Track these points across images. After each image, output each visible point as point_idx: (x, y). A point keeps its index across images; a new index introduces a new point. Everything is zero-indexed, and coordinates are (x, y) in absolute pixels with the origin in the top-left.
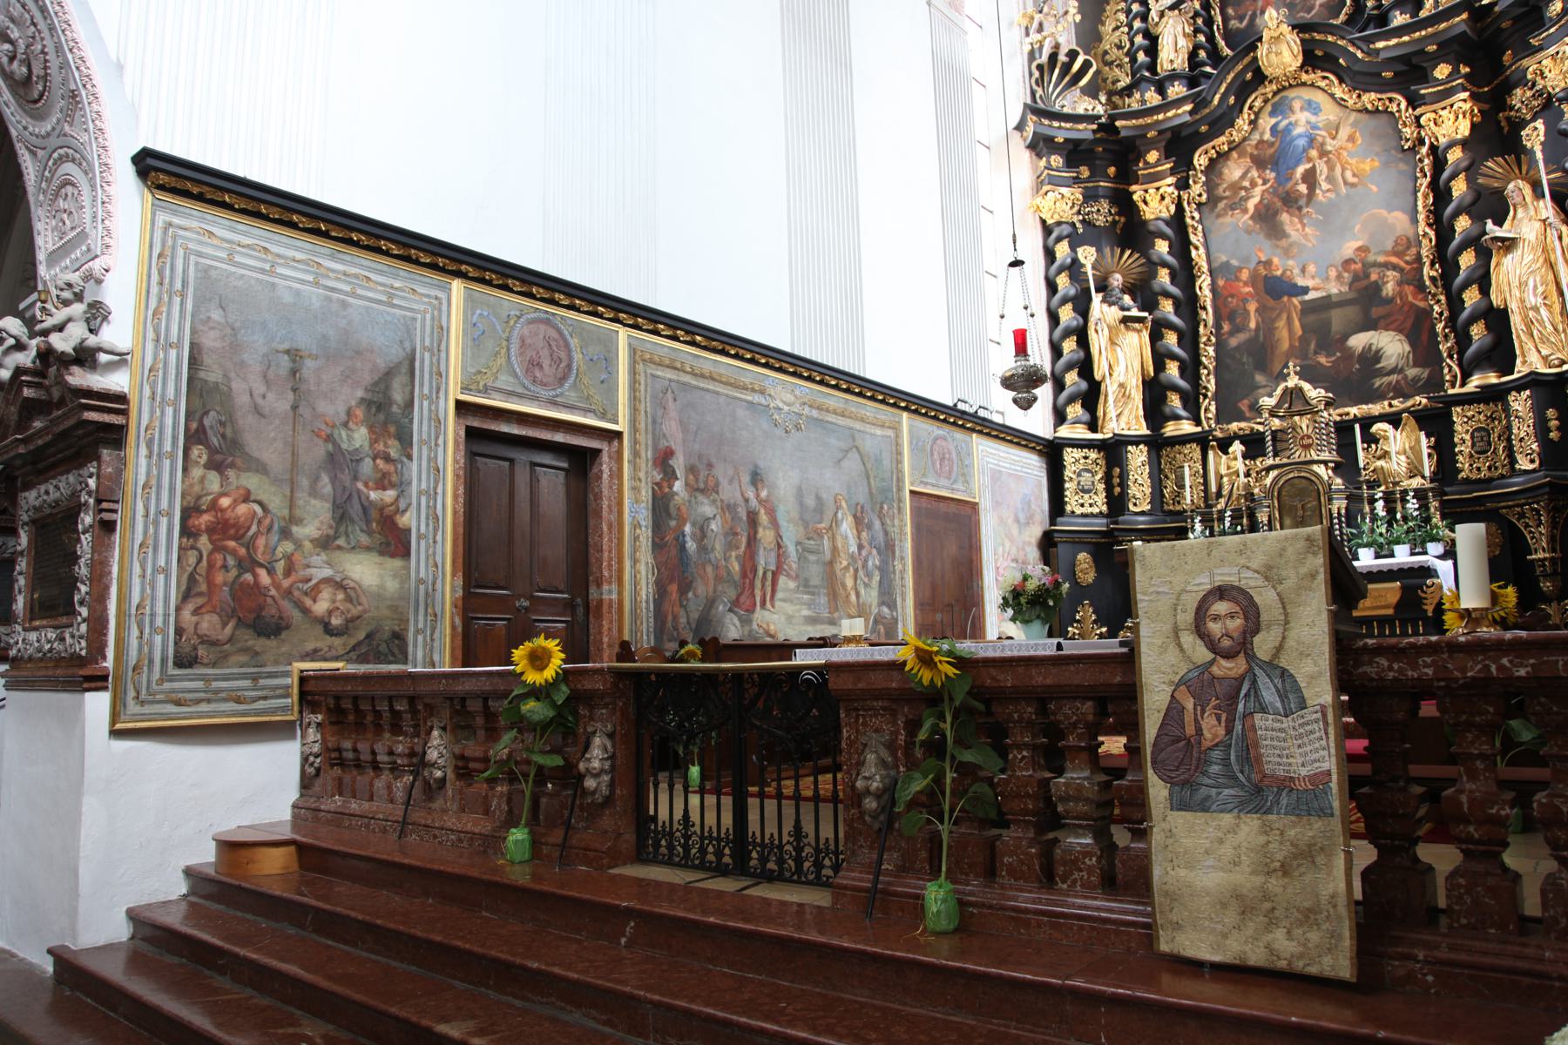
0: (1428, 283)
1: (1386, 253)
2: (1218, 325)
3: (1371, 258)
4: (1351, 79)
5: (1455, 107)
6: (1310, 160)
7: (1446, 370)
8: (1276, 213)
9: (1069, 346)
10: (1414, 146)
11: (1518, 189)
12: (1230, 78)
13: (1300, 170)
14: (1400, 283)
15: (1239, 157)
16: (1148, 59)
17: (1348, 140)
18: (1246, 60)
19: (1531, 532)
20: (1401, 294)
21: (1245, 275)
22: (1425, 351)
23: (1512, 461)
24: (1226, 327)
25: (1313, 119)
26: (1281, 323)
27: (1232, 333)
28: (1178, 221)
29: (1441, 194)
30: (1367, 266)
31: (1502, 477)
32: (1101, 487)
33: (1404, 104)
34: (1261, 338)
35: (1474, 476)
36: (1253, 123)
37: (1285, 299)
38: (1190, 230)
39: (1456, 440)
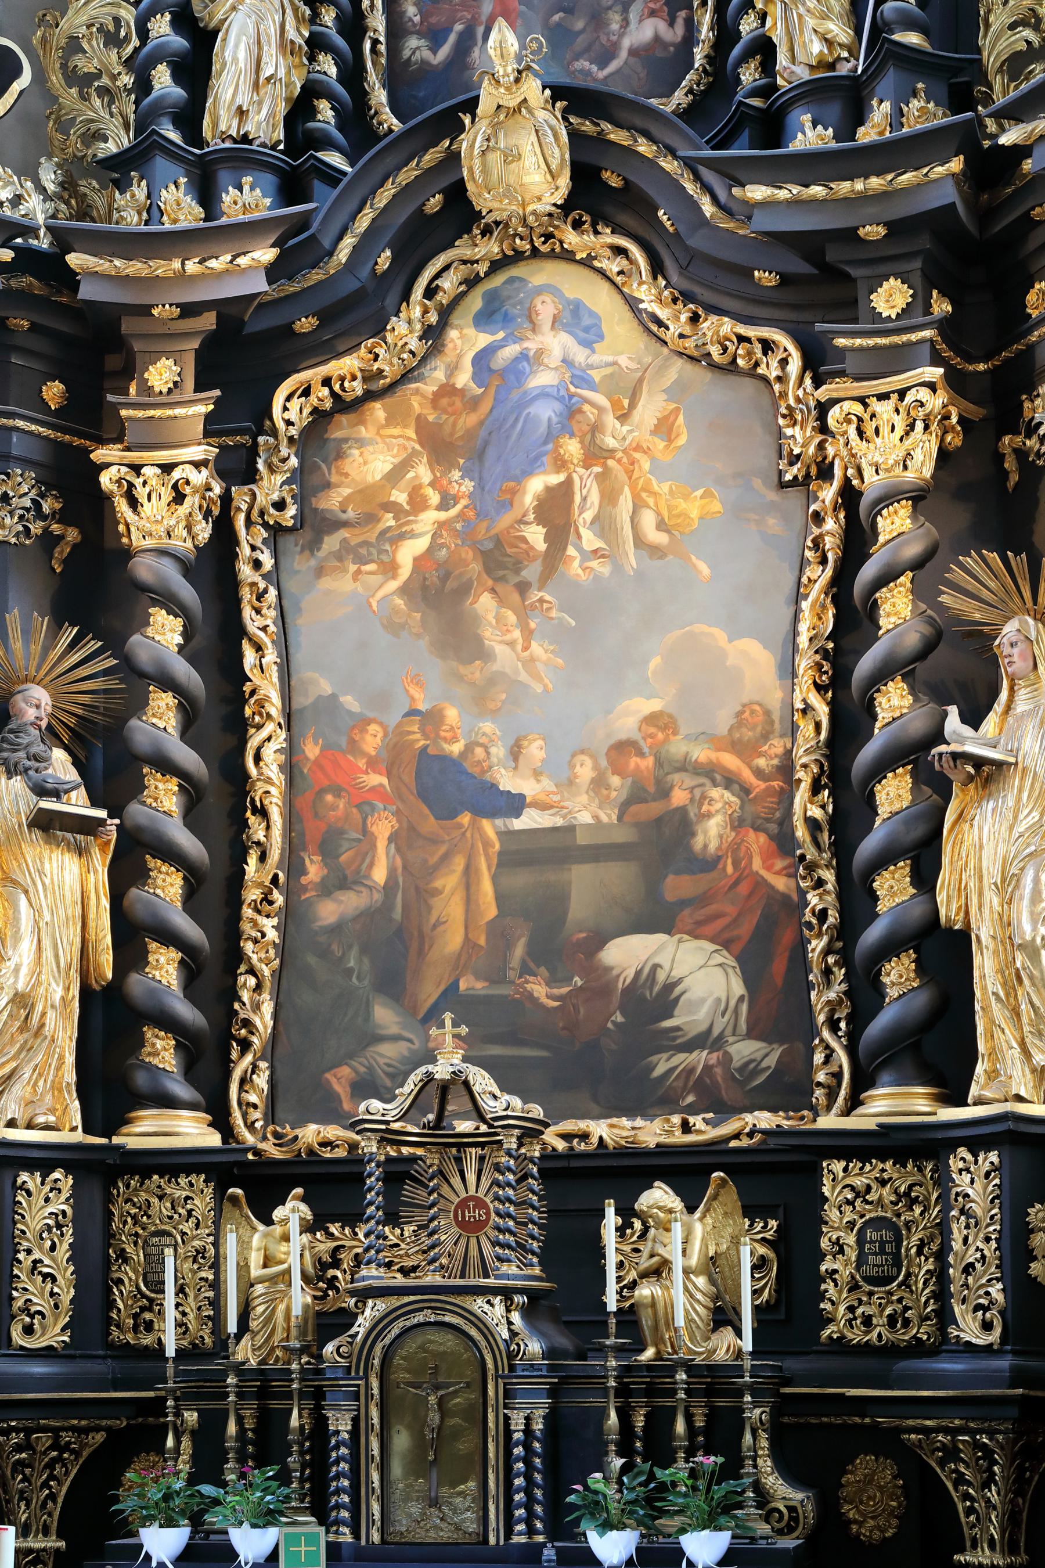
0: (801, 832)
1: (718, 743)
3: (678, 747)
4: (683, 269)
5: (910, 397)
6: (561, 464)
7: (819, 1058)
8: (464, 590)
12: (384, 197)
13: (536, 485)
14: (737, 823)
15: (390, 421)
16: (179, 92)
17: (656, 431)
19: (966, 1496)
20: (735, 848)
21: (372, 740)
24: (314, 870)
25: (580, 355)
26: (449, 881)
27: (329, 888)
31: (917, 1349)
34: (397, 914)
35: (856, 1336)
37: (465, 819)
38: (246, 594)
39: (824, 1244)
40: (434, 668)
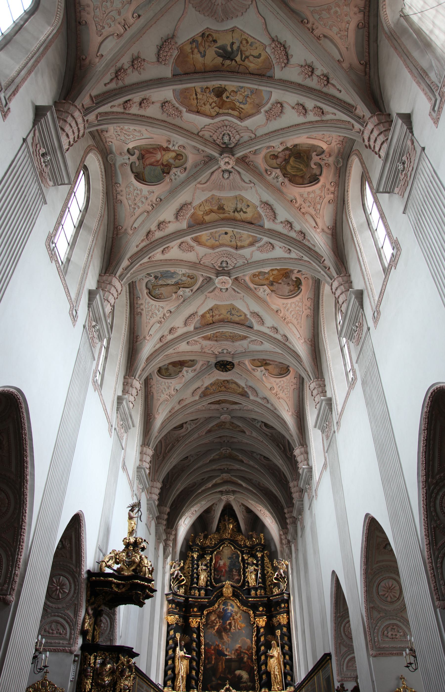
2: (204, 661)
3: (242, 650)
8: (221, 632)
9: (170, 662)
10: (253, 624)
13: (228, 622)
14: (248, 658)
18: (220, 590)
21: (213, 647)
22: (252, 679)
24: (206, 662)
26: (220, 663)
28: (198, 628)
33: (252, 612)
36: (219, 606)
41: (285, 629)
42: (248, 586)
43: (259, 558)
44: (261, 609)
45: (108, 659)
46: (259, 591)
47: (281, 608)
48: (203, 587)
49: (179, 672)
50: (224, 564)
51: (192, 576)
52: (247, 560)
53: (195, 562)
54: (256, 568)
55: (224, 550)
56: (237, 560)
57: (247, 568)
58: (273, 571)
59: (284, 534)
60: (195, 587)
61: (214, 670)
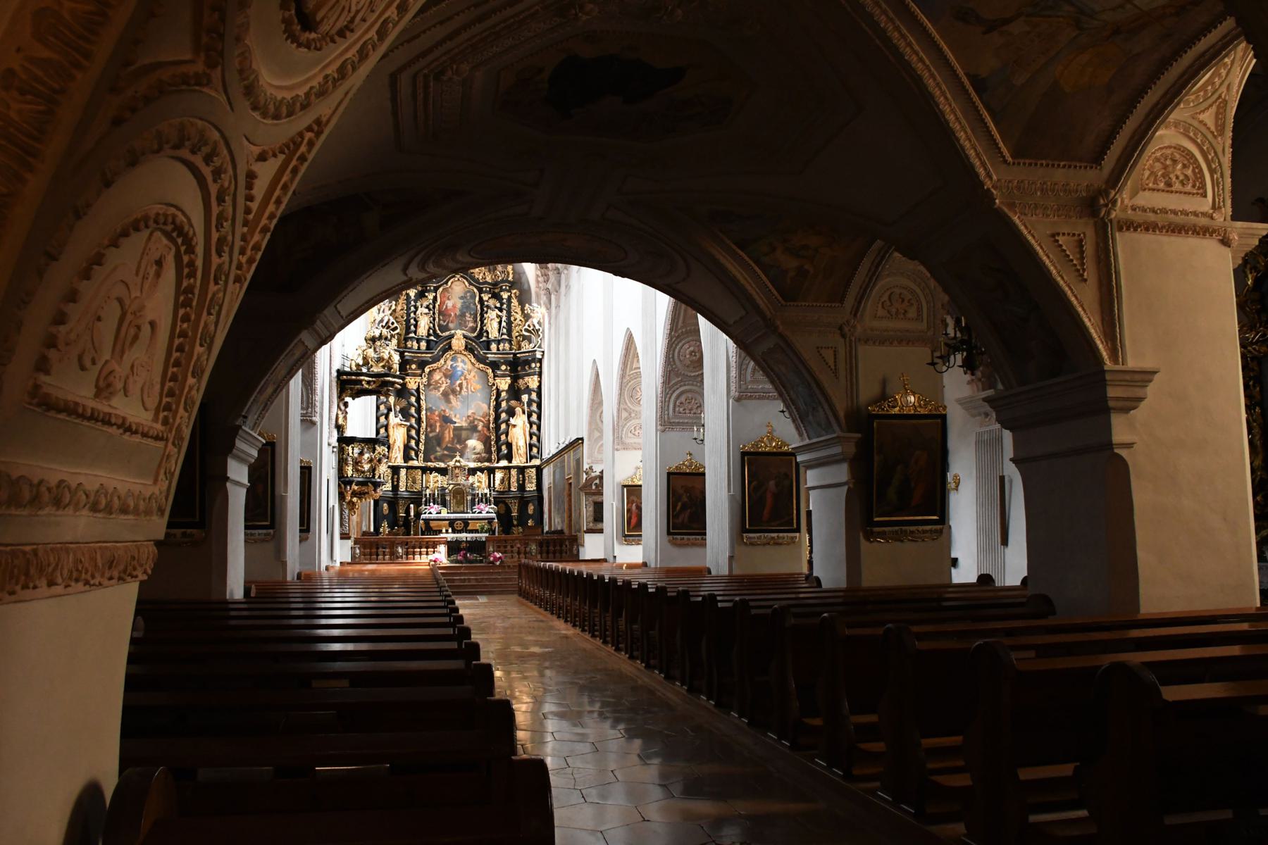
2: (426, 429)
3: (476, 417)
8: (449, 395)
11: (518, 410)
12: (442, 345)
13: (458, 382)
14: (483, 427)
21: (437, 413)
22: (488, 449)
23: (510, 487)
24: (429, 430)
25: (464, 366)
26: (447, 432)
27: (431, 432)
28: (418, 390)
29: (498, 406)
30: (475, 419)
31: (506, 491)
32: (390, 481)
33: (491, 371)
36: (445, 362)
40: (445, 404)
41: (534, 396)
42: (488, 337)
43: (505, 301)
44: (503, 367)
45: (366, 450)
46: (502, 345)
47: (530, 368)
48: (424, 337)
49: (395, 442)
50: (453, 306)
51: (408, 321)
52: (487, 301)
53: (413, 303)
54: (499, 313)
55: (453, 286)
56: (472, 301)
57: (487, 313)
58: (524, 318)
59: (542, 276)
60: (413, 337)
61: (439, 439)
